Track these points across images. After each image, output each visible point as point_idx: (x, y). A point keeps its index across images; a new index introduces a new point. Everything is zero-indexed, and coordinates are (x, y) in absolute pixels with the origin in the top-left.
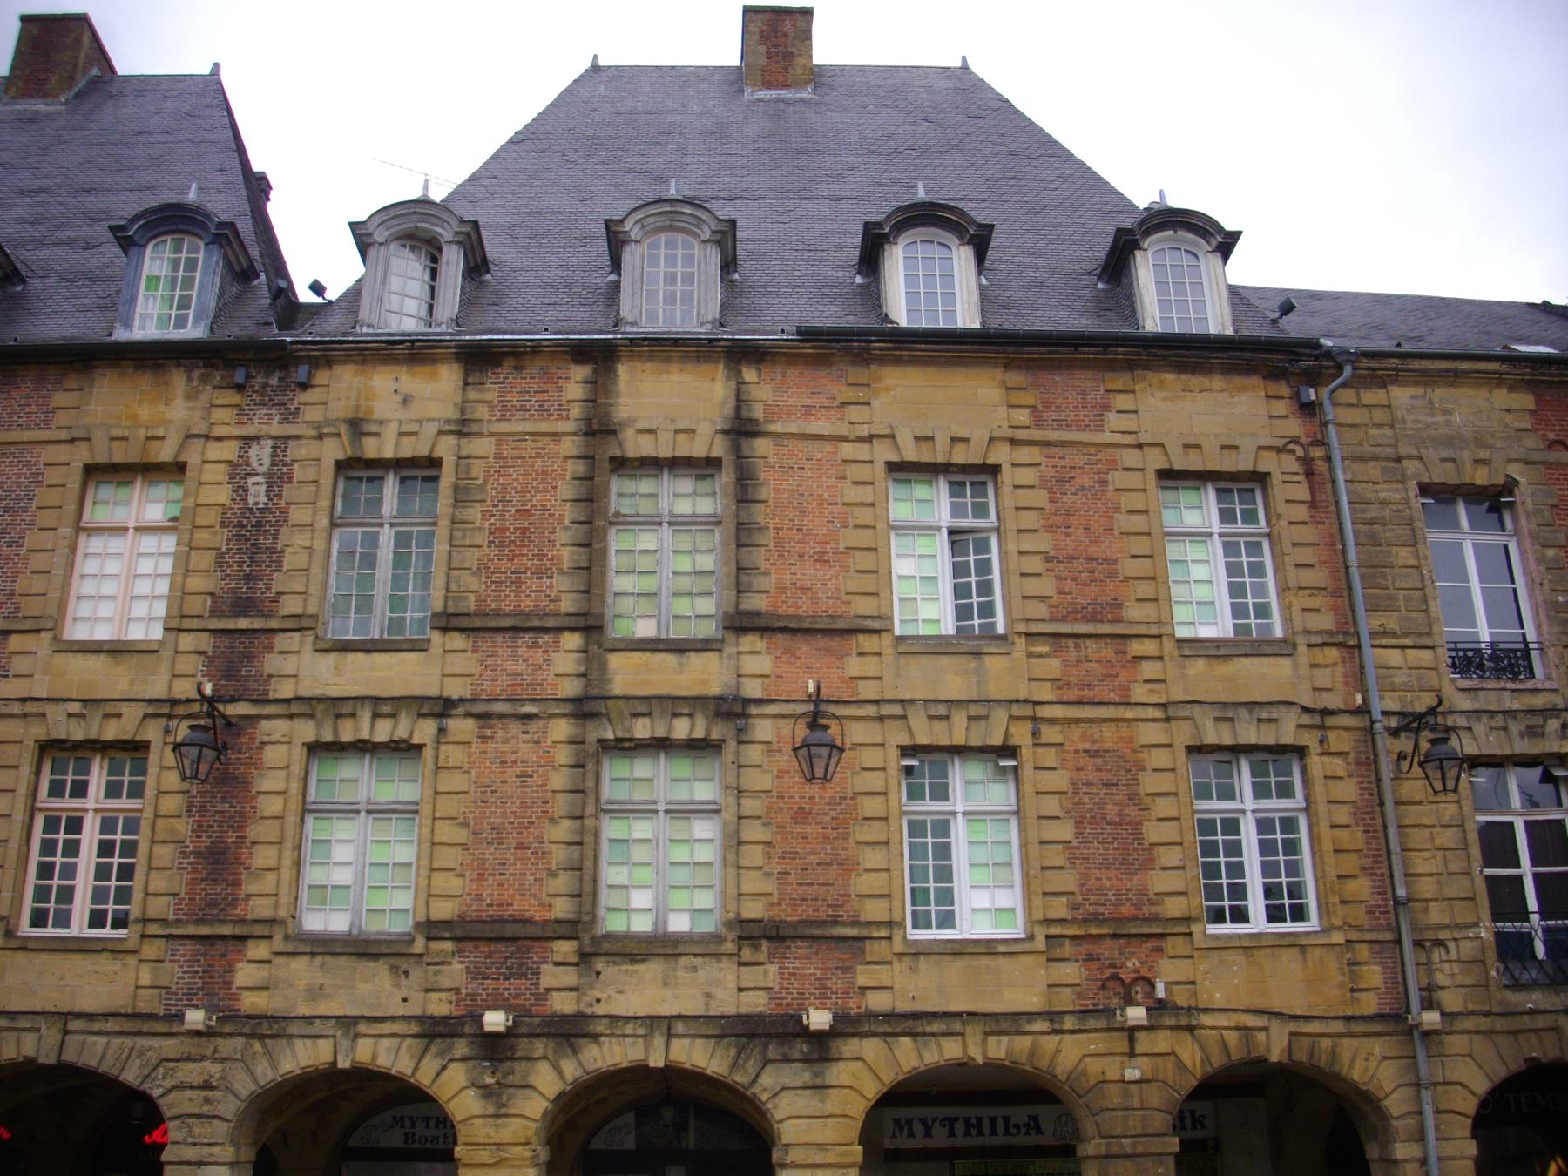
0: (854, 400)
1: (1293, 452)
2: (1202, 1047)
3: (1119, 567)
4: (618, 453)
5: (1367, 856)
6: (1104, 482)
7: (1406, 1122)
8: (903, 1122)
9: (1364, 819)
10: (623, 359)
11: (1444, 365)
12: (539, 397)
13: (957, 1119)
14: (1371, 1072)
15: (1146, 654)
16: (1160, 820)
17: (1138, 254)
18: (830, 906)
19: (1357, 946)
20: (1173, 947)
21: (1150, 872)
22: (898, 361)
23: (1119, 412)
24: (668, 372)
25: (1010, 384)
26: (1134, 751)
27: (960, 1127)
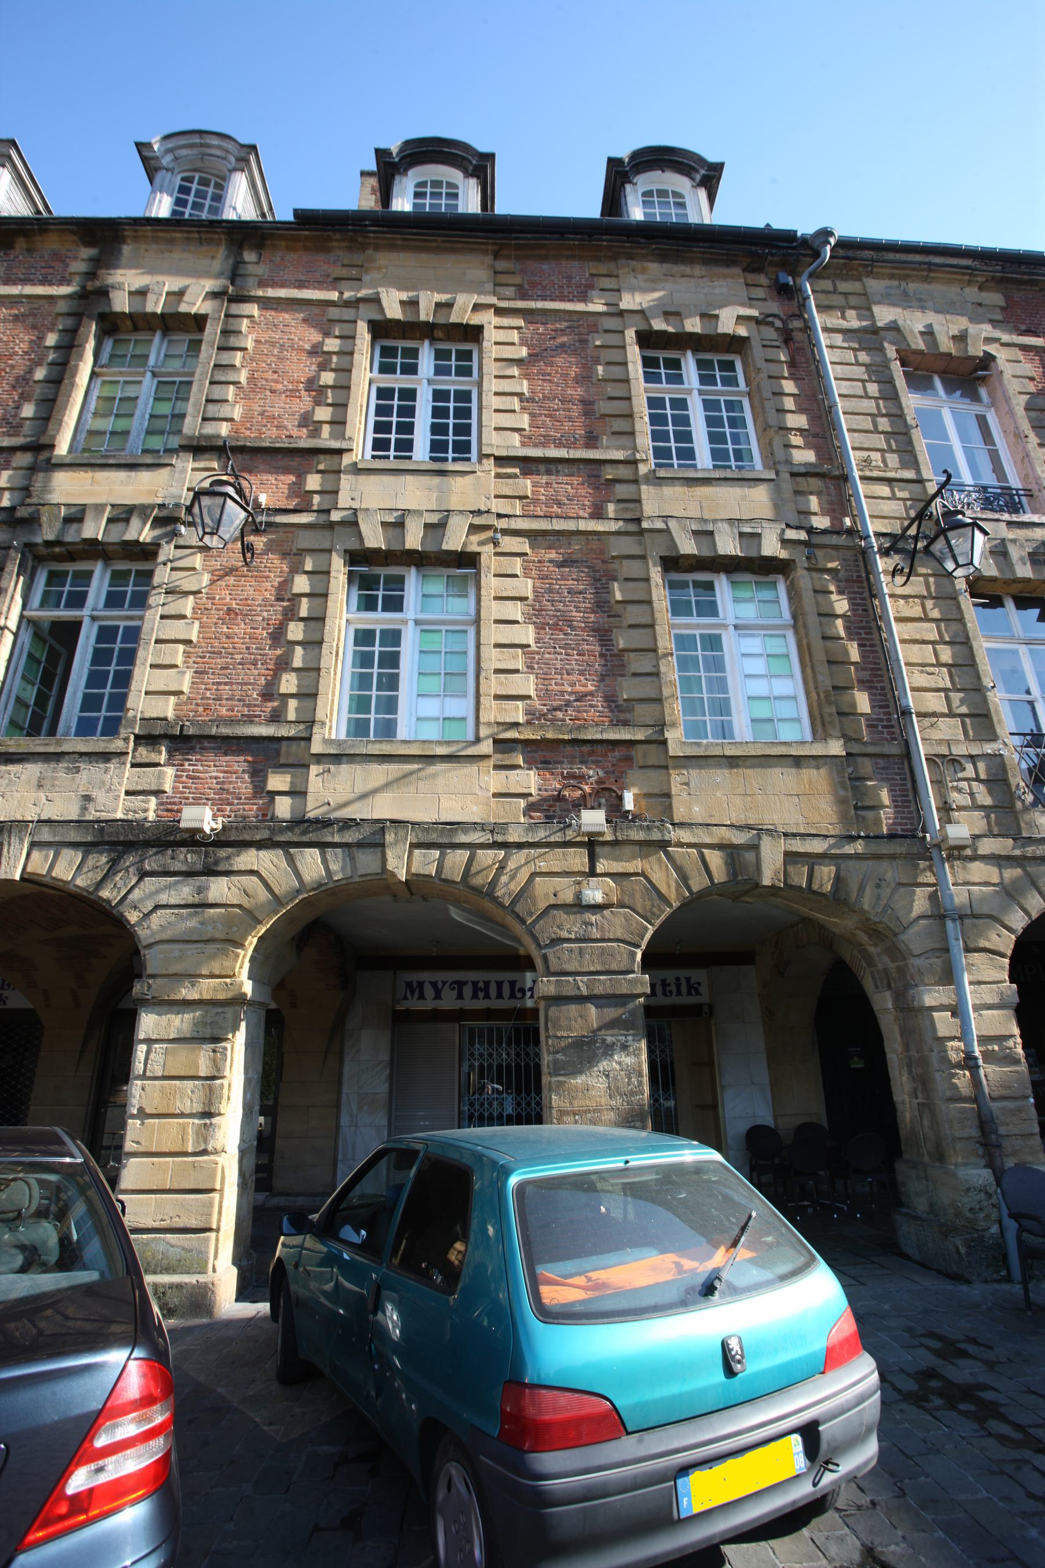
0: (346, 276)
1: (772, 324)
2: (679, 869)
3: (596, 407)
4: (107, 310)
5: (866, 669)
6: (584, 342)
7: (931, 961)
8: (415, 985)
9: (860, 634)
10: (129, 241)
11: (918, 258)
12: (43, 271)
13: (466, 983)
14: (884, 902)
15: (621, 477)
16: (631, 626)
17: (628, 187)
18: (248, 706)
19: (860, 760)
20: (644, 756)
21: (619, 679)
22: (393, 247)
23: (602, 290)
24: (171, 251)
25: (499, 269)
26: (604, 562)
27: (468, 990)
